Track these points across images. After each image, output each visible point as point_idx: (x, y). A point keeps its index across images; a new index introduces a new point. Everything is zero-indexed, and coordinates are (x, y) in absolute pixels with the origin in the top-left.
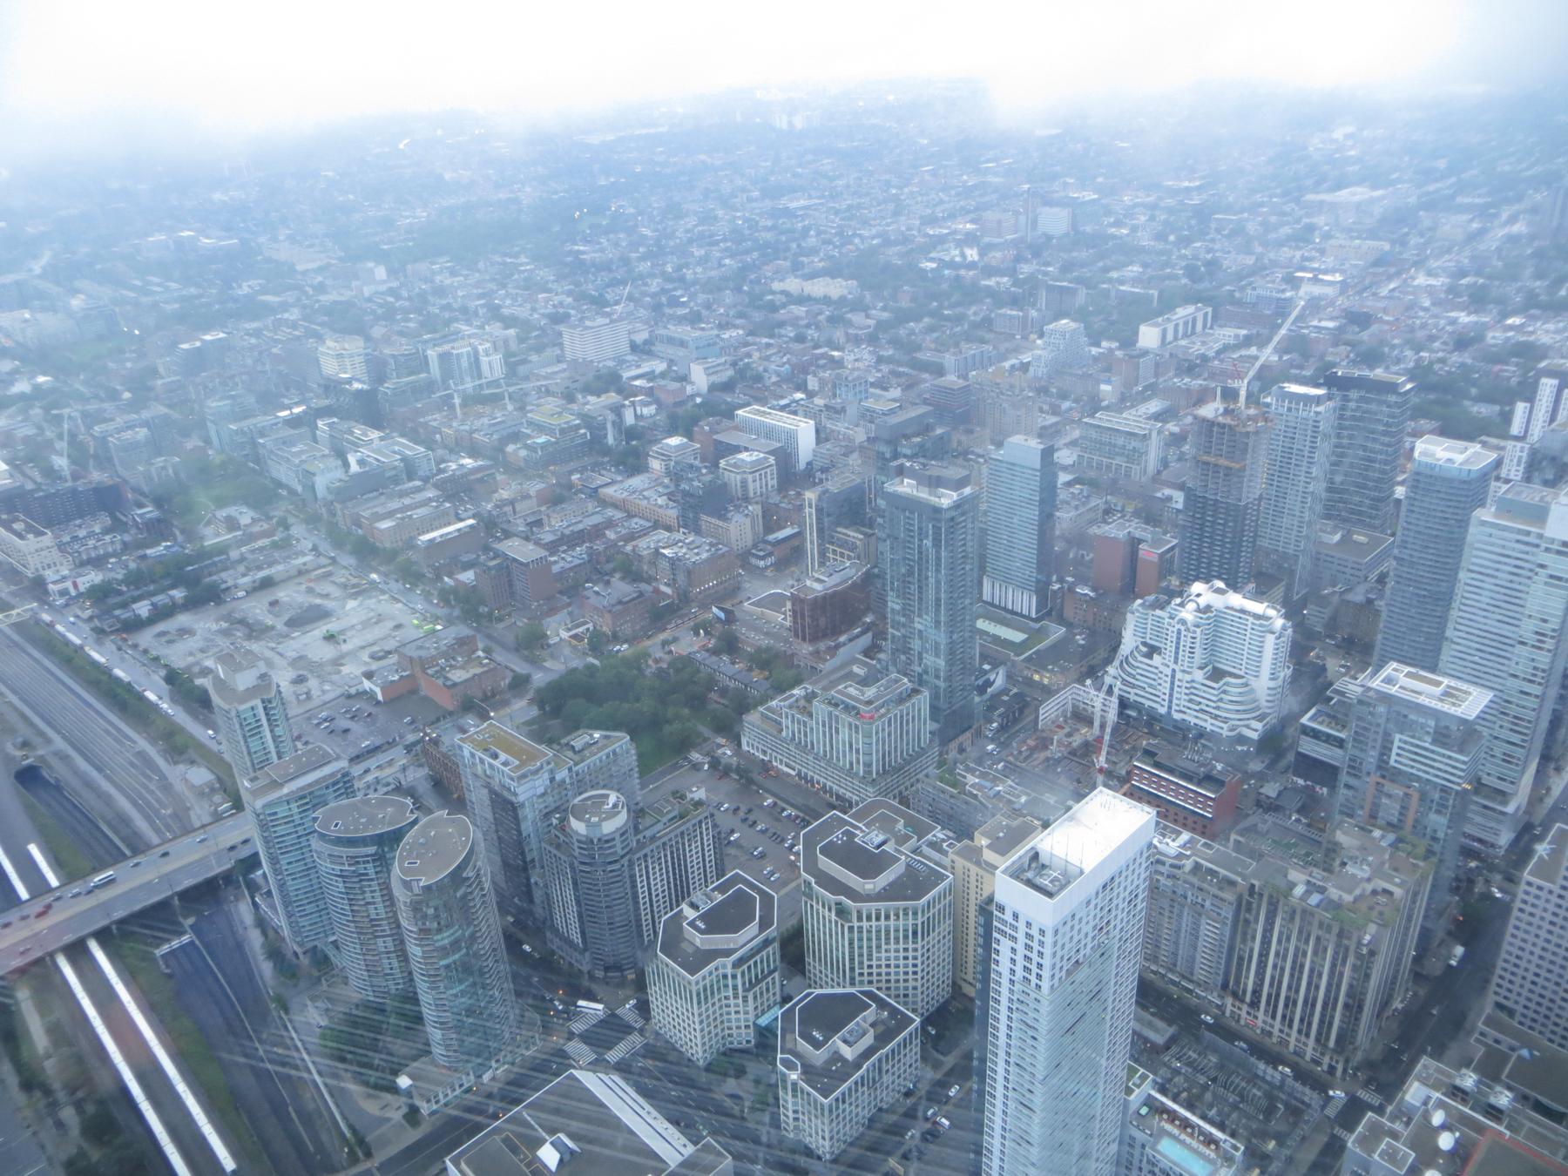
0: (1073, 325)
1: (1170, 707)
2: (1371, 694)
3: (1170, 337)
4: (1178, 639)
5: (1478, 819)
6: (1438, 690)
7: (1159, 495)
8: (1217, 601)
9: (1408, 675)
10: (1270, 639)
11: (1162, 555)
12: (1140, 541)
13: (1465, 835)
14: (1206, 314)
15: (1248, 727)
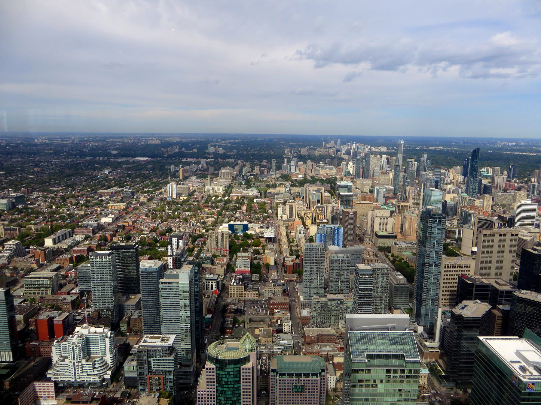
0: (17, 242)
1: (75, 378)
2: (141, 348)
3: (57, 241)
4: (73, 350)
5: (184, 377)
6: (159, 340)
7: (60, 298)
8: (85, 332)
9: (151, 338)
10: (107, 340)
11: (63, 321)
12: (54, 318)
13: (181, 384)
14: (69, 232)
15: (106, 374)
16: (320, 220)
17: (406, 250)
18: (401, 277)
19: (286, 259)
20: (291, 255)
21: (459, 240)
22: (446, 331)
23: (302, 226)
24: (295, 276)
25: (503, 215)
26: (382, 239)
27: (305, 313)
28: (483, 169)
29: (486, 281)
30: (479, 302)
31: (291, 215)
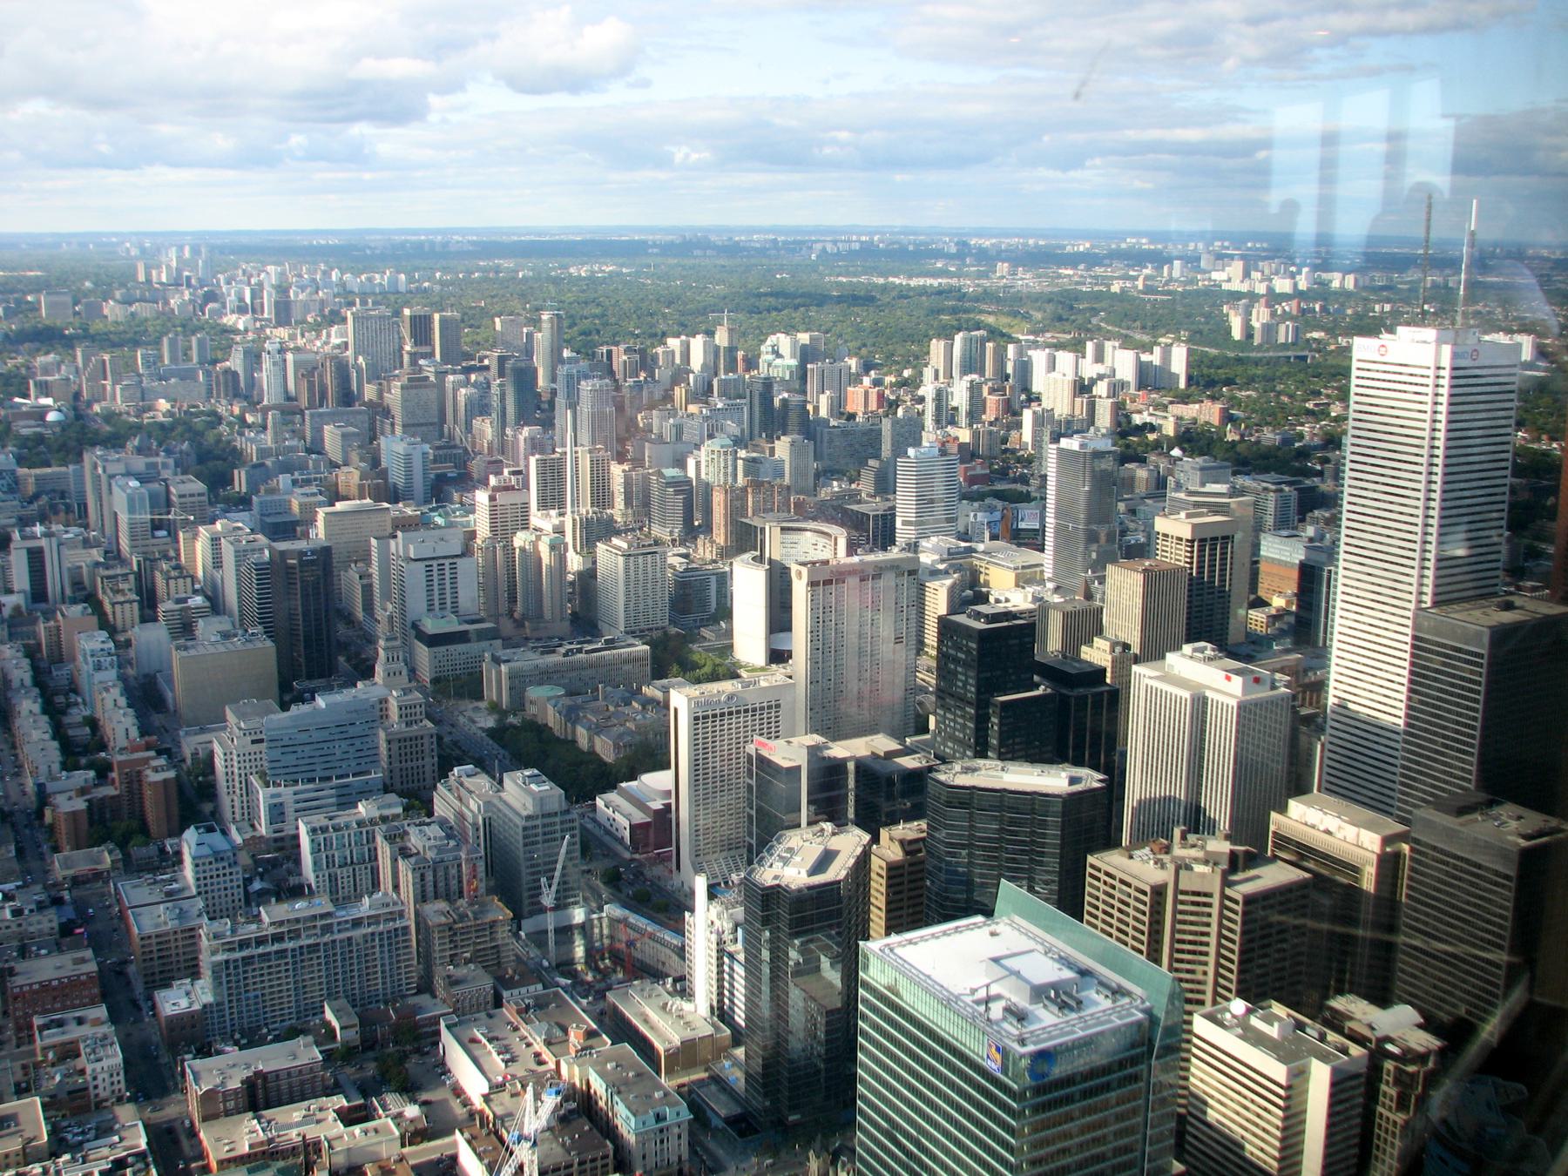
16: (178, 601)
17: (545, 676)
18: (546, 787)
19: (50, 787)
20: (65, 767)
21: (726, 613)
22: (731, 956)
23: (104, 635)
24: (106, 857)
25: (855, 507)
26: (443, 649)
27: (176, 1001)
28: (769, 342)
29: (839, 750)
30: (828, 827)
31: (38, 593)
